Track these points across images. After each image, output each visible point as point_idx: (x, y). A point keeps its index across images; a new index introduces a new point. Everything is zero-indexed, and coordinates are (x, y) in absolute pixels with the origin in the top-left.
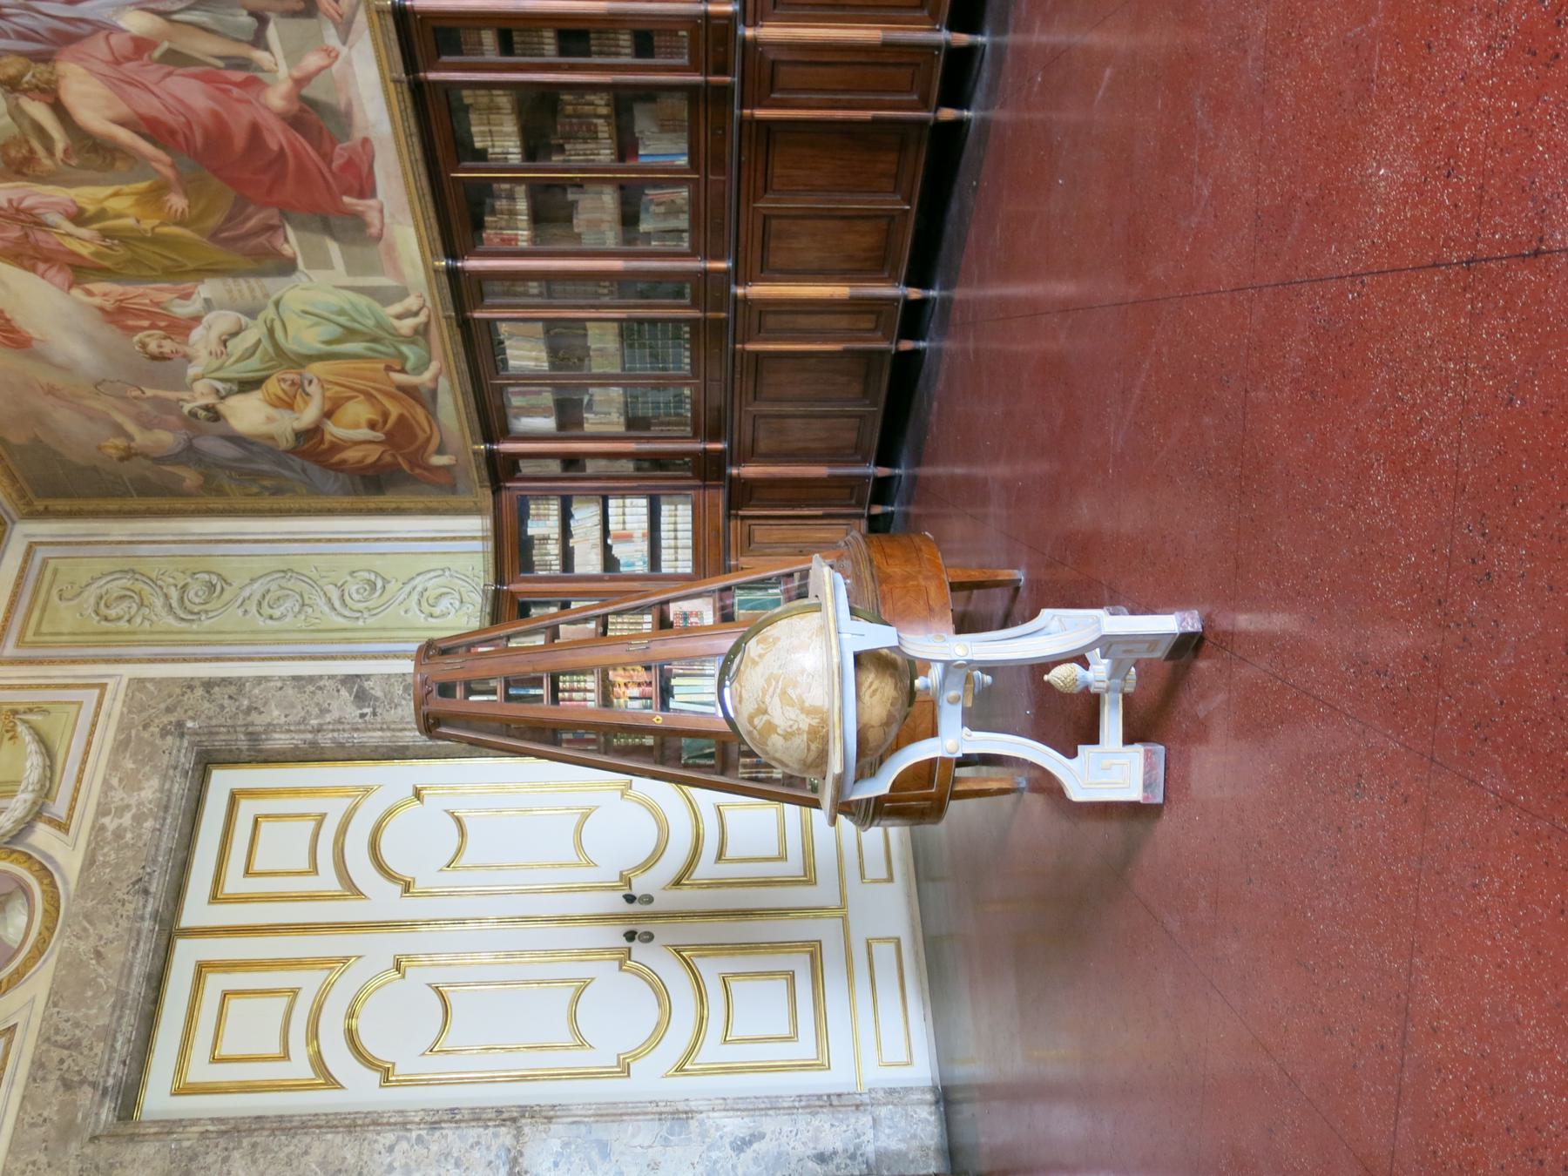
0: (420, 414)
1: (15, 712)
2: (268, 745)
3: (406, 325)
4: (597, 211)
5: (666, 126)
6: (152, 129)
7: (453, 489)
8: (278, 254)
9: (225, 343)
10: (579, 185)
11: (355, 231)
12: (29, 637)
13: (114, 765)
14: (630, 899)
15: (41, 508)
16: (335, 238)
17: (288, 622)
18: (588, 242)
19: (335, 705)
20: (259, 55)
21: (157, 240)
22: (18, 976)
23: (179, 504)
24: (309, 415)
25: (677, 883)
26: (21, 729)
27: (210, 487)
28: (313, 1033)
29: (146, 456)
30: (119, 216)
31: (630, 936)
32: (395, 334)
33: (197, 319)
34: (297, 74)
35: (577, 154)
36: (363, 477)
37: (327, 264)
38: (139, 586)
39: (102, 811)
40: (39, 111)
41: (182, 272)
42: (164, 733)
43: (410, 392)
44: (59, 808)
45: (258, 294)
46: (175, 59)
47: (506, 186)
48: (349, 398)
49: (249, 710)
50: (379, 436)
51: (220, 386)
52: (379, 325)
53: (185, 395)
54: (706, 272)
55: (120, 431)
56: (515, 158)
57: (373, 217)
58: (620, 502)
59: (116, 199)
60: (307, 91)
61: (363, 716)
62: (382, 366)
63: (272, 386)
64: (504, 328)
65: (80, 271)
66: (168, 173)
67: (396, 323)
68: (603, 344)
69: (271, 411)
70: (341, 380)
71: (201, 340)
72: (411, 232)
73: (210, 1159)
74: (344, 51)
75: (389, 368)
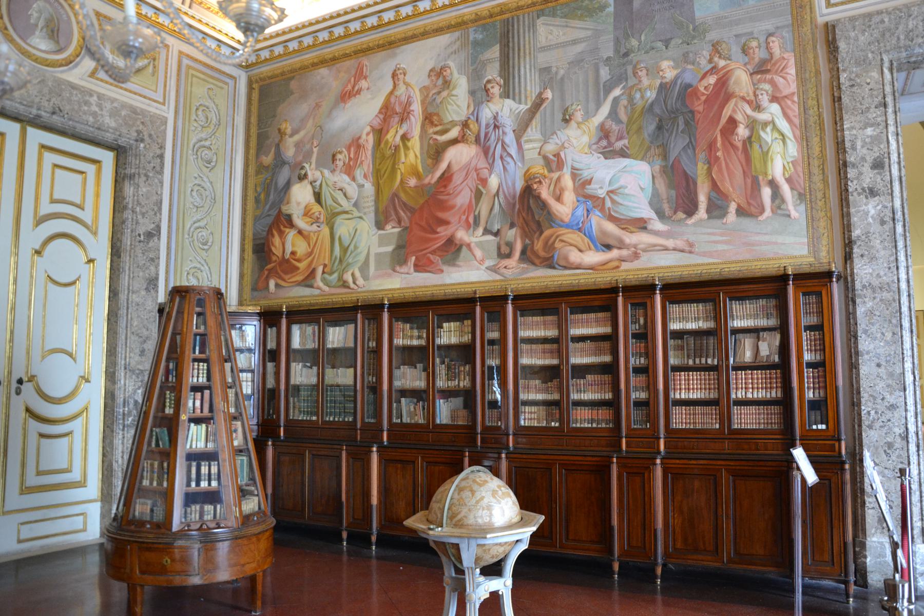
0: (299, 278)
1: (154, 59)
2: (127, 183)
3: (348, 277)
4: (410, 378)
6: (446, 178)
7: (254, 289)
8: (387, 221)
10: (425, 369)
12: (191, 72)
13: (124, 106)
14: (20, 381)
15: (254, 86)
16: (394, 250)
18: (397, 373)
19: (146, 221)
20: (480, 230)
21: (394, 170)
23: (253, 152)
24: (300, 223)
25: (28, 410)
27: (261, 168)
29: (280, 141)
30: (406, 155)
32: (344, 271)
33: (354, 179)
34: (473, 245)
36: (264, 244)
37: (381, 244)
38: (212, 127)
39: (100, 97)
40: (454, 133)
41: (377, 176)
42: (139, 132)
43: (312, 274)
45: (366, 210)
46: (478, 195)
47: (425, 335)
49: (146, 176)
51: (318, 183)
52: (348, 265)
53: (313, 166)
55: (295, 132)
56: (438, 341)
57: (404, 269)
58: (250, 379)
59: (413, 156)
60: (464, 249)
61: (139, 235)
62: (326, 262)
63: (316, 208)
64: (351, 327)
65: (379, 133)
66: (426, 181)
67: (350, 273)
68: (343, 376)
69: (303, 206)
70: (319, 242)
71: (343, 179)
72: (398, 286)
74: (483, 267)
75: (325, 266)
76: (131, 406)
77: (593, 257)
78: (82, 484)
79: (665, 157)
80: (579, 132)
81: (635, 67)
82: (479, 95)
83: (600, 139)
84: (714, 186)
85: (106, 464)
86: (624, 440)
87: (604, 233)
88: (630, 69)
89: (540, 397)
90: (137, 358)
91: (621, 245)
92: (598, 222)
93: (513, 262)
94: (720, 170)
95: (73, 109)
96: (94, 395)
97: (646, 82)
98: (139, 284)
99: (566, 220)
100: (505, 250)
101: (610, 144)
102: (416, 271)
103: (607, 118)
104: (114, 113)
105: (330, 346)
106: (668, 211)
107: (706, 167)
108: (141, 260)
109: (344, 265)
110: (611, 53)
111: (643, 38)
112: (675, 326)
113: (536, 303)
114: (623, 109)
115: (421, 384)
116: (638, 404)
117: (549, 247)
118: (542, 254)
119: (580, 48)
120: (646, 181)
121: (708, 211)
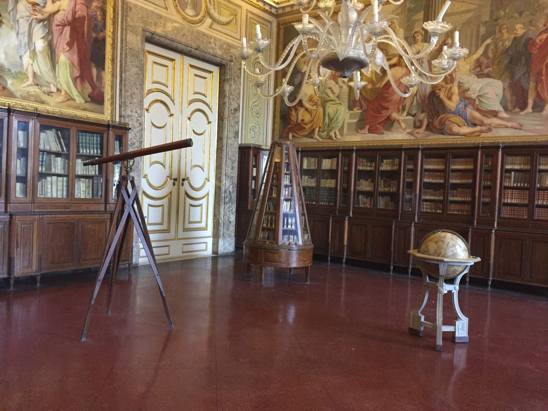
0: (306, 133)
1: (236, 15)
2: (226, 84)
4: (365, 186)
5: (386, 204)
8: (354, 107)
9: (330, 88)
10: (372, 182)
11: (359, 126)
12: (252, 21)
13: (225, 43)
14: (183, 180)
16: (359, 121)
17: (251, 90)
18: (357, 182)
19: (234, 103)
20: (405, 113)
22: (179, 12)
24: (307, 105)
25: (186, 193)
26: (232, 17)
28: (159, 91)
31: (174, 179)
32: (330, 131)
33: (337, 83)
34: (400, 121)
35: (381, 182)
37: (350, 118)
39: (215, 39)
43: (313, 131)
44: (215, 26)
45: (343, 100)
47: (374, 165)
48: (311, 116)
49: (234, 80)
50: (299, 121)
52: (333, 128)
54: (350, 210)
56: (381, 169)
57: (363, 131)
60: (396, 122)
64: (335, 160)
66: (377, 86)
67: (333, 132)
68: (330, 183)
69: (309, 95)
72: (359, 140)
73: (137, 62)
74: (405, 132)
75: (320, 128)
76: (228, 193)
77: (466, 130)
78: (205, 229)
79: (512, 77)
80: (465, 63)
81: (500, 28)
82: (410, 40)
83: (476, 67)
84: (538, 95)
85: (215, 220)
86: (476, 221)
87: (473, 117)
88: (497, 28)
89: (432, 198)
90: (231, 171)
91: (482, 124)
92: (470, 112)
93: (421, 131)
94: (543, 86)
95: (204, 47)
96: (210, 188)
97: (506, 36)
98: (231, 135)
99: (453, 110)
100: (418, 124)
101: (482, 70)
102: (369, 133)
103: (481, 55)
104: (221, 47)
105: (323, 168)
106: (510, 106)
107: (534, 85)
108: (232, 123)
109: (330, 128)
110: (487, 19)
111: (507, 11)
112: (508, 167)
113: (432, 152)
114: (491, 51)
115: (368, 189)
116: (484, 204)
117: (442, 123)
118: (438, 127)
119: (470, 15)
120: (500, 91)
121: (533, 108)
